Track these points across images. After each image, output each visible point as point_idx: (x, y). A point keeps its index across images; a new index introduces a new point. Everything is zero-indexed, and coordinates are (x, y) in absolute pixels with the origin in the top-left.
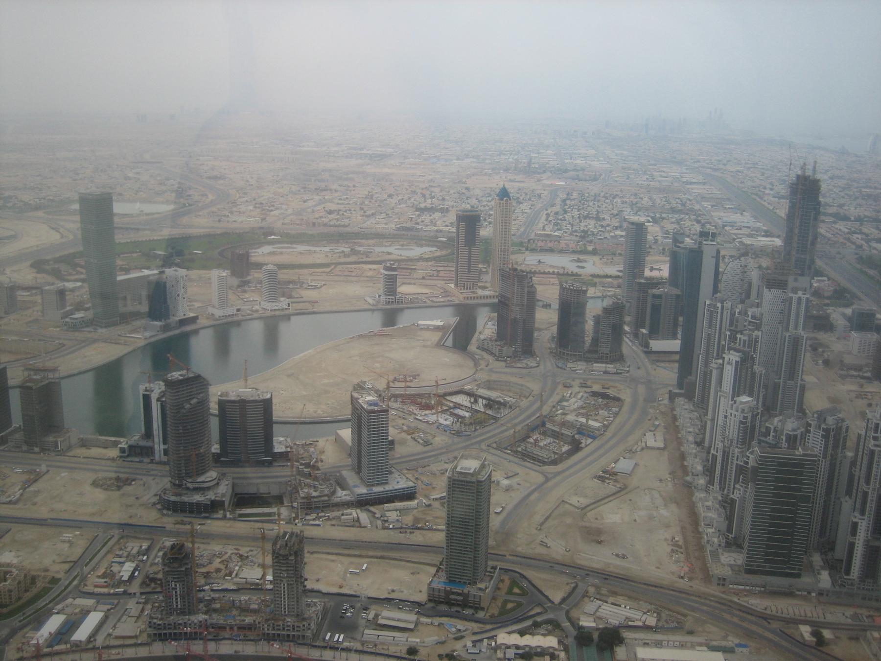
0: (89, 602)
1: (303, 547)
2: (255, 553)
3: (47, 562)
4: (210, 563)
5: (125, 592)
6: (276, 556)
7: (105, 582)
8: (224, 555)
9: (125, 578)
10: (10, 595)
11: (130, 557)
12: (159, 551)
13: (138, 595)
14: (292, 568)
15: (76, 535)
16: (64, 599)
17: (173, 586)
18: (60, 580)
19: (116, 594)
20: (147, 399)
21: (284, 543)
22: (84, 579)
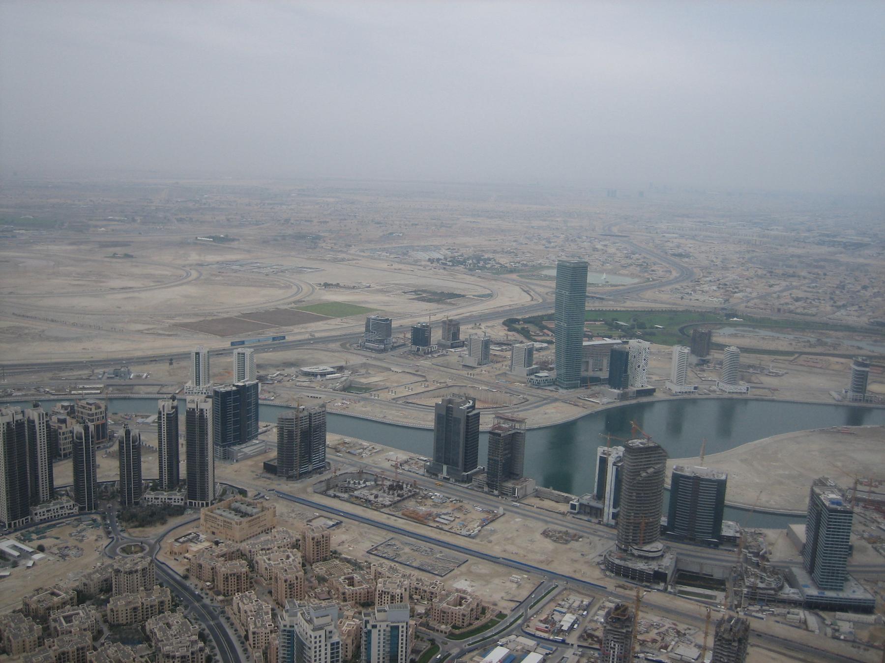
0: (531, 643)
1: (748, 636)
2: (692, 632)
3: (496, 597)
4: (647, 632)
5: (563, 642)
6: (719, 638)
7: (546, 627)
8: (661, 627)
9: (565, 628)
10: (463, 619)
11: (571, 610)
12: (599, 609)
13: (575, 646)
14: (734, 655)
15: (523, 578)
16: (509, 634)
17: (612, 645)
18: (506, 616)
19: (556, 641)
20: (604, 461)
21: (729, 627)
22: (527, 620)
